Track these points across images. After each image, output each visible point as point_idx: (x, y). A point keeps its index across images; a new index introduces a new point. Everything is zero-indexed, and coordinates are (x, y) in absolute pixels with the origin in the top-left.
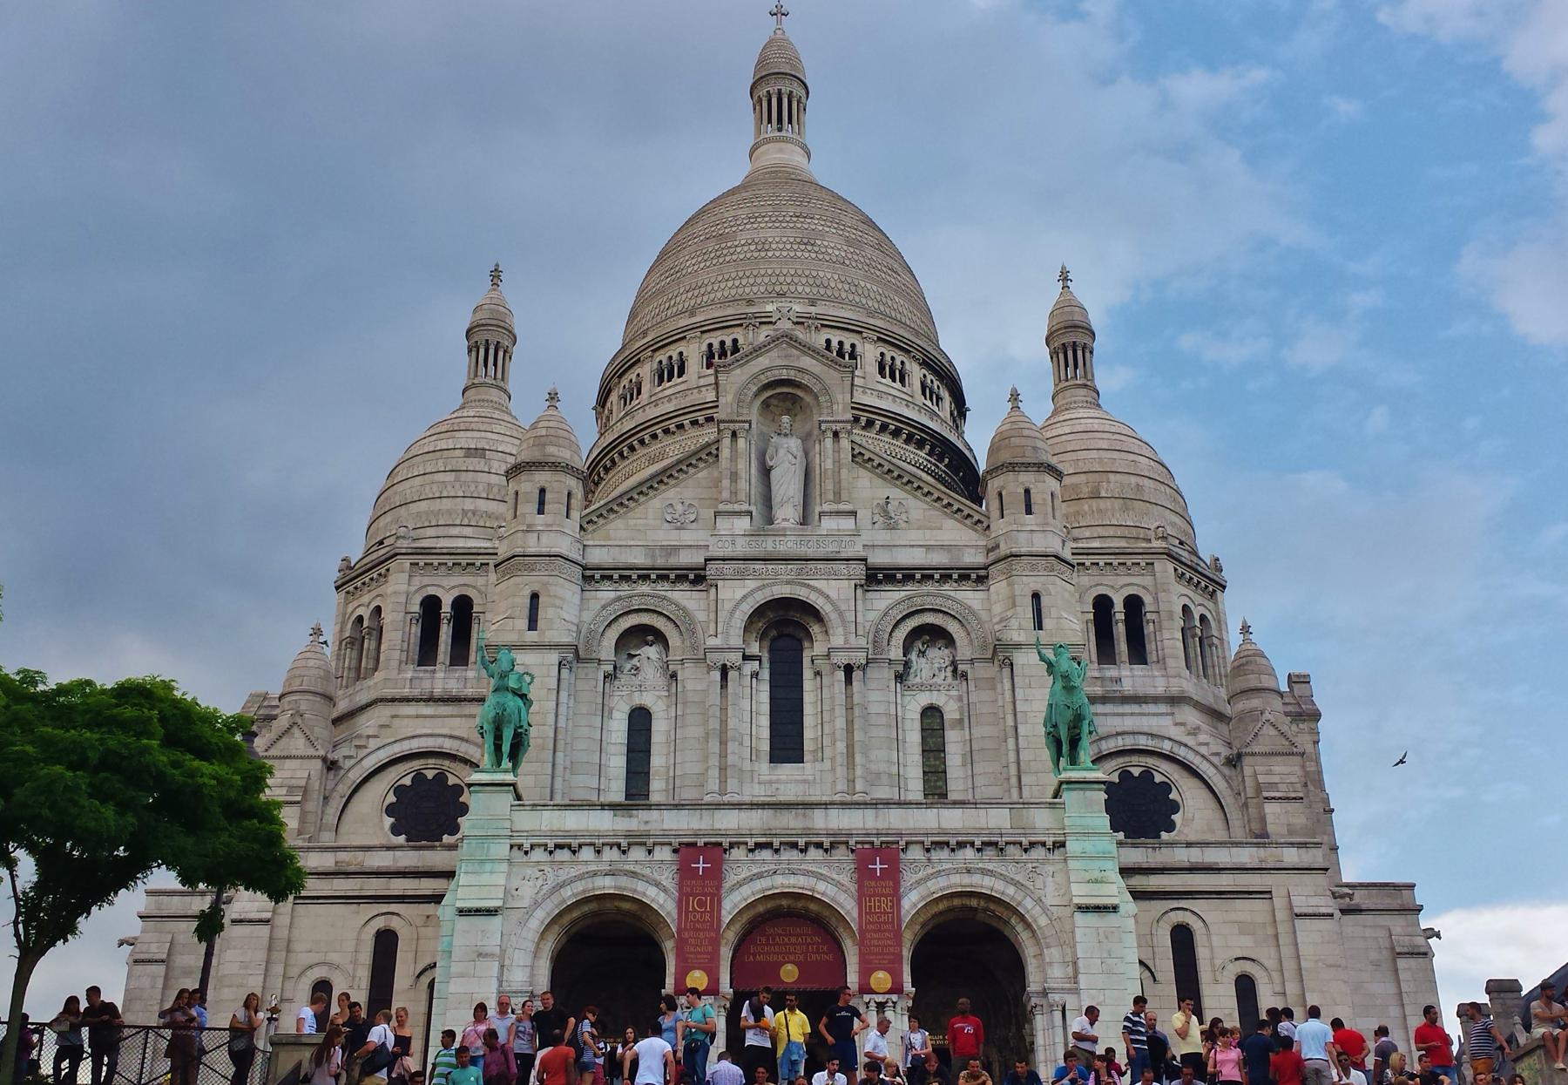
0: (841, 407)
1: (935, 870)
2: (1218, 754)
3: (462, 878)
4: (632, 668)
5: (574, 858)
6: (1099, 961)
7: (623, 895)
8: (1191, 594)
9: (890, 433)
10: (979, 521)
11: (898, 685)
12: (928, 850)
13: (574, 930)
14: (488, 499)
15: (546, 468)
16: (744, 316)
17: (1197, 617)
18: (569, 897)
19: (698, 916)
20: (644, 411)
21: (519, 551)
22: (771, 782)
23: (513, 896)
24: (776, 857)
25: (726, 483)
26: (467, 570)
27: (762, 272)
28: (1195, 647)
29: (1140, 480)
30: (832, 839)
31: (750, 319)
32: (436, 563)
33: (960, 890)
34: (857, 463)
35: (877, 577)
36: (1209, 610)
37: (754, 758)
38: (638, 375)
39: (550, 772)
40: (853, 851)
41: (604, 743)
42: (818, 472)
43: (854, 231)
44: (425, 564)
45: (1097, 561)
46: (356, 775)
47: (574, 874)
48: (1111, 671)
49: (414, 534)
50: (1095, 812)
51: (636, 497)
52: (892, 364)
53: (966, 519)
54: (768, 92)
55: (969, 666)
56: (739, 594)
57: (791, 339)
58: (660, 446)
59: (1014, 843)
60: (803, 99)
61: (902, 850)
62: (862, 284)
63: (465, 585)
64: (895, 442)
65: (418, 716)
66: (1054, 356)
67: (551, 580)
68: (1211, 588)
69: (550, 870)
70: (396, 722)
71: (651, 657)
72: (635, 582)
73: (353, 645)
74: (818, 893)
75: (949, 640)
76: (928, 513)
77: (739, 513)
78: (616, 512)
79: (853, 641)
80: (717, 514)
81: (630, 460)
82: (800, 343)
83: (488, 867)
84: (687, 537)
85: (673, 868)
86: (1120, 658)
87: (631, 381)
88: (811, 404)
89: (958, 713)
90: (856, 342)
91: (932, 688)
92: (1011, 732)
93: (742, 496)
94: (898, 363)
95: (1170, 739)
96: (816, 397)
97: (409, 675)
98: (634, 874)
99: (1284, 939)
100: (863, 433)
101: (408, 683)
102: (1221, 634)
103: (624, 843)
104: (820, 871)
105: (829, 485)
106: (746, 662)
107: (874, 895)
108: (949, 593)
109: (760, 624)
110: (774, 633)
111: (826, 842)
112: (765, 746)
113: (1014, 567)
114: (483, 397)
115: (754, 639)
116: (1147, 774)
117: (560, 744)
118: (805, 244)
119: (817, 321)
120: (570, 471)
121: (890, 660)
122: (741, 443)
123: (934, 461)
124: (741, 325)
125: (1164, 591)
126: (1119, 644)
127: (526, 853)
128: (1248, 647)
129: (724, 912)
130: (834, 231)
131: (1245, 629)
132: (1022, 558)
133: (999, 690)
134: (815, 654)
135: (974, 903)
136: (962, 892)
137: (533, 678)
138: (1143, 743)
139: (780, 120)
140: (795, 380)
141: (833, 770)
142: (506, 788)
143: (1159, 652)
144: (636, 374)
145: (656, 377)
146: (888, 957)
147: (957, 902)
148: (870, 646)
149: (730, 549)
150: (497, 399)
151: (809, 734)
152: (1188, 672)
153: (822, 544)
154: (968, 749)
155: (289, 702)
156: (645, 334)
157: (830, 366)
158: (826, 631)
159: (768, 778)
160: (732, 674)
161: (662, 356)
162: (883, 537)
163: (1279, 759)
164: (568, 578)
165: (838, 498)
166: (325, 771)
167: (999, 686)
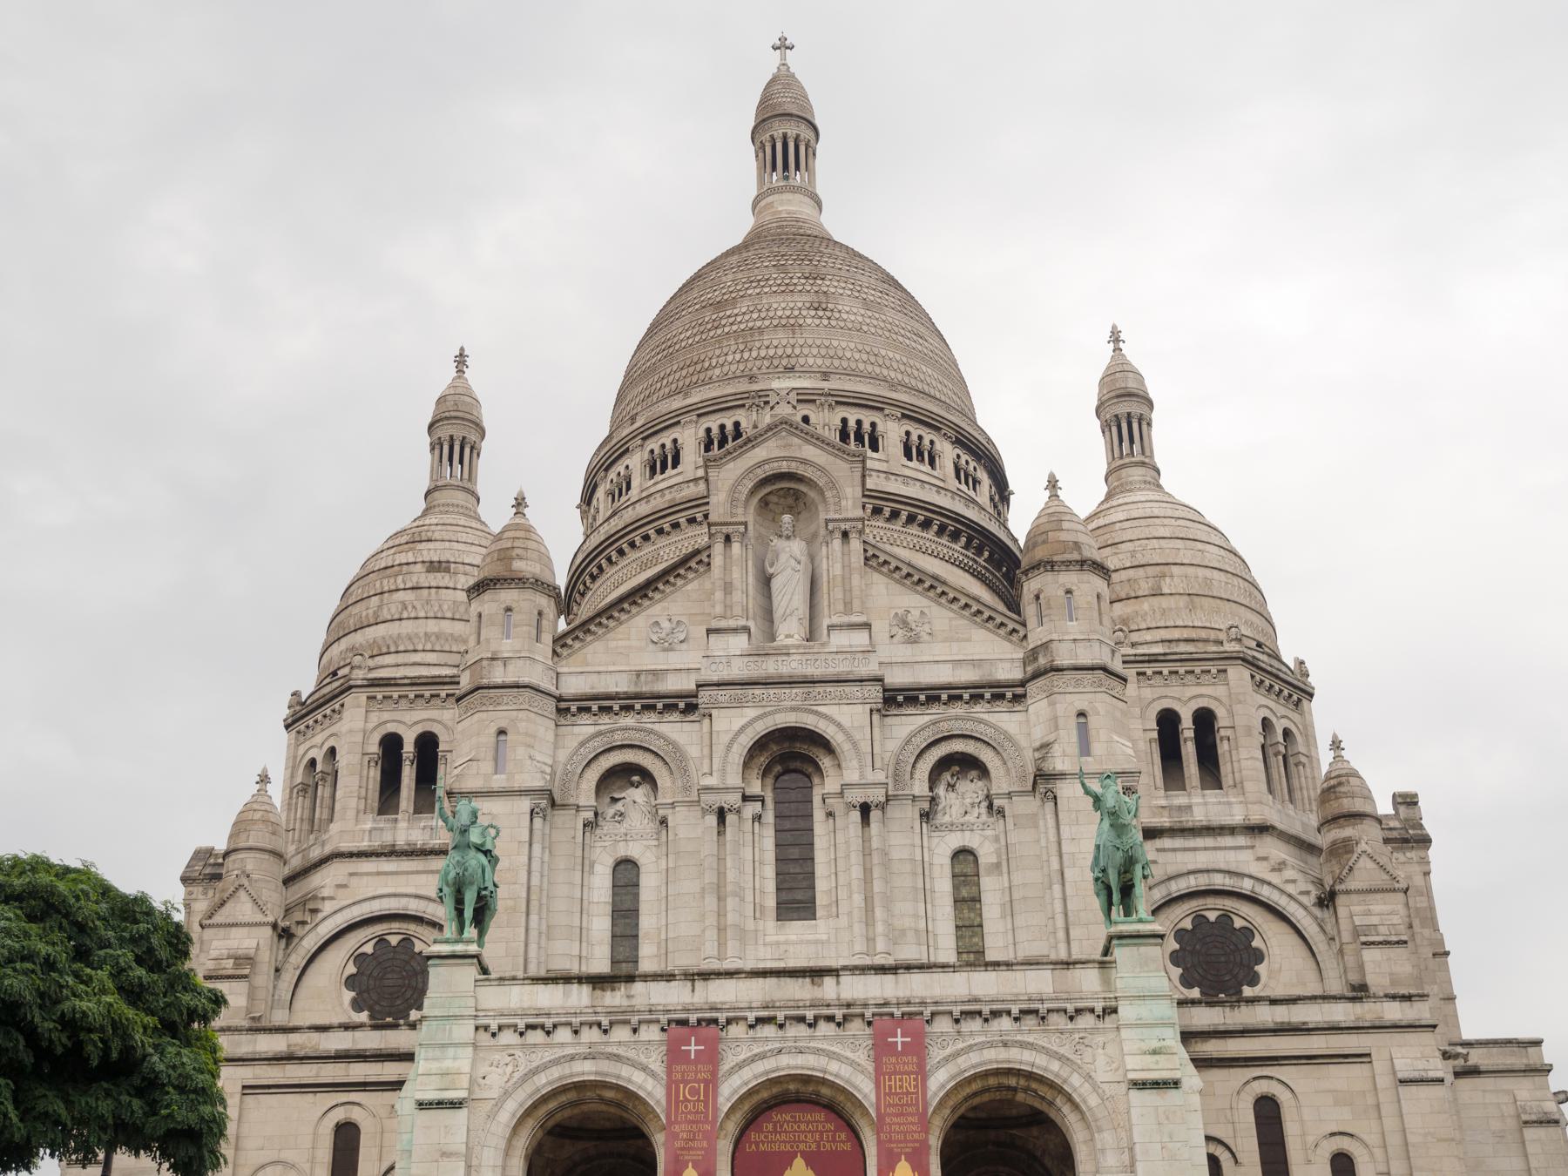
0: (850, 502)
1: (965, 1044)
2: (1308, 893)
3: (422, 1064)
4: (616, 814)
5: (548, 1040)
6: (1159, 1146)
7: (605, 1082)
8: (1272, 704)
9: (920, 525)
10: (1014, 630)
11: (924, 825)
12: (957, 1021)
13: (550, 1124)
14: (453, 619)
15: (513, 586)
16: (746, 395)
17: (1280, 732)
18: (544, 1086)
19: (690, 1106)
20: (634, 508)
21: (485, 681)
22: (778, 943)
23: (479, 1085)
24: (780, 1033)
25: (719, 595)
26: (432, 702)
27: (766, 343)
28: (1278, 767)
29: (1208, 572)
30: (845, 1011)
31: (753, 398)
32: (395, 695)
33: (995, 1066)
34: (871, 567)
35: (896, 699)
36: (1295, 723)
37: (758, 915)
38: (627, 467)
39: (522, 937)
40: (869, 1024)
41: (585, 903)
43: (873, 292)
44: (384, 697)
45: (1159, 669)
46: (310, 943)
47: (548, 1059)
48: (1179, 799)
49: (371, 663)
50: (1151, 971)
52: (920, 444)
53: (999, 628)
54: (772, 137)
55: (1006, 801)
56: (737, 723)
57: (791, 425)
58: (653, 548)
59: (1058, 1011)
60: (812, 142)
61: (927, 1021)
62: (883, 352)
63: (424, 720)
64: (924, 535)
65: (379, 874)
66: (1106, 430)
67: (522, 715)
68: (1295, 697)
69: (521, 1054)
70: (354, 880)
71: (638, 800)
72: (616, 714)
73: (306, 792)
74: (831, 1074)
75: (983, 771)
77: (735, 630)
78: (594, 633)
79: (872, 777)
80: (709, 632)
81: (620, 566)
83: (451, 1051)
84: (675, 660)
85: (660, 1050)
86: (1191, 783)
87: (619, 474)
89: (995, 855)
90: (877, 421)
91: (964, 827)
92: (1056, 878)
93: (737, 610)
94: (926, 442)
95: (1251, 877)
96: (821, 492)
97: (369, 825)
98: (617, 1058)
99: (1388, 1109)
100: (888, 526)
101: (367, 833)
102: (1309, 750)
103: (605, 1022)
104: (832, 1049)
105: (838, 594)
106: (747, 803)
107: (895, 1073)
108: (981, 716)
109: (762, 759)
110: (778, 768)
111: (839, 1014)
112: (771, 902)
113: (1055, 683)
114: (449, 501)
115: (755, 776)
116: (1226, 917)
117: (534, 904)
118: (816, 309)
119: (830, 398)
120: (540, 588)
121: (914, 797)
122: (736, 547)
123: (971, 555)
124: (743, 406)
125: (1240, 702)
126: (1188, 766)
127: (494, 1035)
128: (1340, 765)
129: (721, 1100)
130: (849, 293)
131: (1336, 745)
132: (1065, 673)
133: (1042, 829)
134: (826, 791)
135: (1012, 1082)
136: (997, 1069)
137: (498, 833)
138: (1219, 881)
139: (786, 167)
141: (851, 926)
142: (469, 961)
143: (1236, 775)
144: (625, 465)
145: (648, 469)
146: (912, 1145)
147: (992, 1081)
148: (890, 781)
149: (725, 673)
150: (461, 503)
151: (822, 885)
152: (1270, 797)
154: (1008, 899)
155: (234, 861)
156: (633, 419)
157: (836, 456)
158: (839, 766)
159: (775, 938)
160: (730, 818)
161: (653, 444)
162: (903, 652)
163: (1378, 896)
164: (540, 712)
166: (276, 939)
167: (1041, 823)
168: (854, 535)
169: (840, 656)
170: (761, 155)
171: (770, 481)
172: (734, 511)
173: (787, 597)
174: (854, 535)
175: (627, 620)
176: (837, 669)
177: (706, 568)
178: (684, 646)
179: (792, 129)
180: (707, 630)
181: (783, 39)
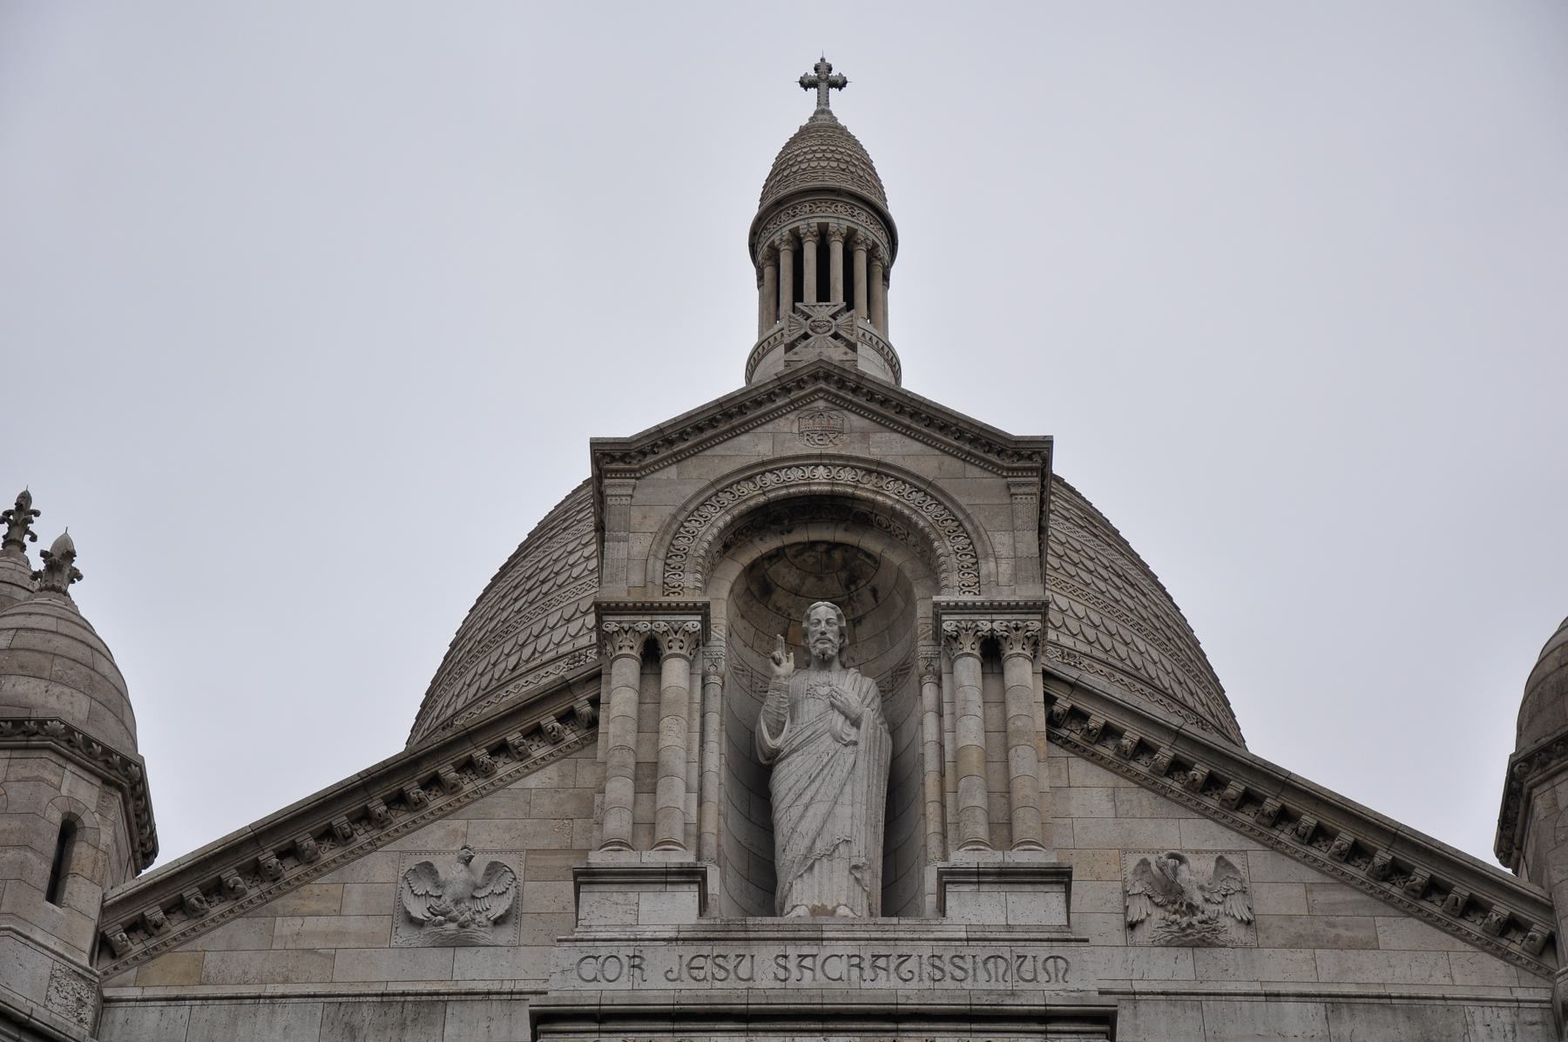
0: (1005, 568)
25: (620, 789)
34: (1066, 743)
42: (931, 764)
51: (308, 842)
57: (841, 383)
60: (883, 252)
76: (1321, 897)
82: (871, 396)
88: (908, 574)
120: (78, 755)
122: (675, 672)
140: (853, 498)
149: (624, 984)
153: (948, 968)
157: (966, 458)
165: (1003, 831)
168: (1018, 649)
169: (982, 952)
170: (769, 271)
171: (777, 520)
172: (674, 580)
173: (819, 809)
174: (1018, 649)
175: (336, 864)
176: (968, 985)
177: (582, 733)
178: (505, 934)
179: (839, 219)
180: (576, 875)
181: (823, 68)
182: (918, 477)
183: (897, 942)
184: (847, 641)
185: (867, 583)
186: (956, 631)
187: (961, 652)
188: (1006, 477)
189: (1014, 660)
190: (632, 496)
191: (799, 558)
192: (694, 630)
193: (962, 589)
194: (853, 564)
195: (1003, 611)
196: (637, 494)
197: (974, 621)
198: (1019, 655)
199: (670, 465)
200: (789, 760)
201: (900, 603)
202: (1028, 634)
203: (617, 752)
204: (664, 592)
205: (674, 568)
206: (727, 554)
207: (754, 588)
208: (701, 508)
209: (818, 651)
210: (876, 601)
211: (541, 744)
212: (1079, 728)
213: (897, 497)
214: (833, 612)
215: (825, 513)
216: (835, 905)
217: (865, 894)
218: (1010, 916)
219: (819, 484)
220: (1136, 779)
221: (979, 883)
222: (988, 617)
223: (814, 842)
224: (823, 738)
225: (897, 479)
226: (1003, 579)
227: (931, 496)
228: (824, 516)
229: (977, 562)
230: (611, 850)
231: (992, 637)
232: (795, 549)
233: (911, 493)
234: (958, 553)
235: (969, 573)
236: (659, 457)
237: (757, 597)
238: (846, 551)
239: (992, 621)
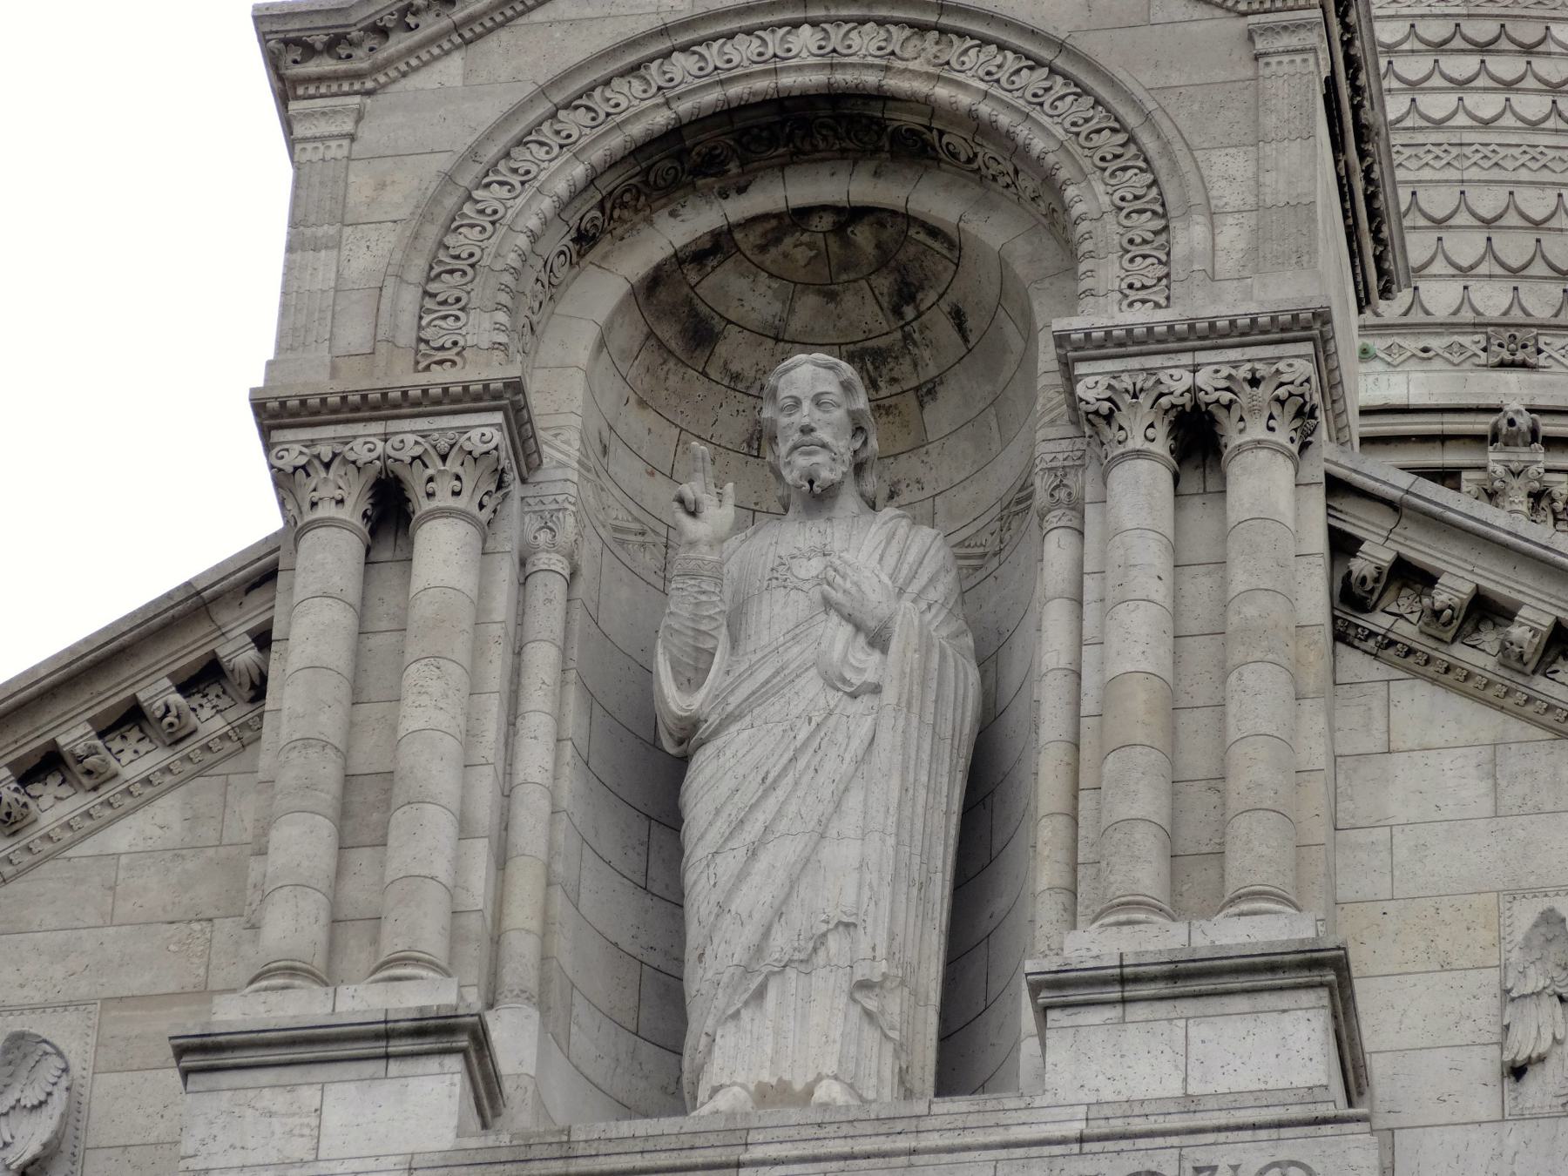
0: (1232, 236)
88: (1020, 268)
140: (883, 97)
168: (1257, 430)
171: (711, 165)
172: (444, 333)
173: (782, 854)
182: (1033, 34)
183: (914, 1159)
184: (874, 443)
185: (941, 296)
186: (1109, 400)
187: (1121, 449)
188: (1244, 14)
189: (1247, 458)
190: (352, 138)
191: (774, 252)
192: (485, 448)
193: (1126, 296)
194: (901, 256)
195: (1220, 341)
196: (367, 133)
197: (1150, 372)
198: (1259, 444)
199: (447, 53)
200: (719, 742)
201: (1016, 343)
202: (1282, 392)
203: (294, 754)
204: (417, 363)
205: (444, 303)
206: (589, 257)
207: (668, 332)
208: (515, 152)
209: (796, 474)
210: (966, 340)
211: (144, 746)
212: (1417, 607)
213: (983, 86)
214: (830, 375)
215: (825, 138)
216: (811, 1077)
217: (889, 1047)
218: (1195, 1074)
219: (799, 68)
220: (1549, 718)
221: (1124, 1001)
222: (1186, 359)
223: (767, 933)
224: (800, 682)
225: (985, 41)
226: (1226, 264)
227: (1065, 76)
228: (822, 145)
229: (1166, 228)
230: (266, 989)
231: (1196, 406)
232: (759, 229)
233: (1018, 71)
234: (1121, 209)
235: (1145, 257)
236: (417, 37)
237: (678, 352)
238: (882, 225)
239: (1195, 369)
